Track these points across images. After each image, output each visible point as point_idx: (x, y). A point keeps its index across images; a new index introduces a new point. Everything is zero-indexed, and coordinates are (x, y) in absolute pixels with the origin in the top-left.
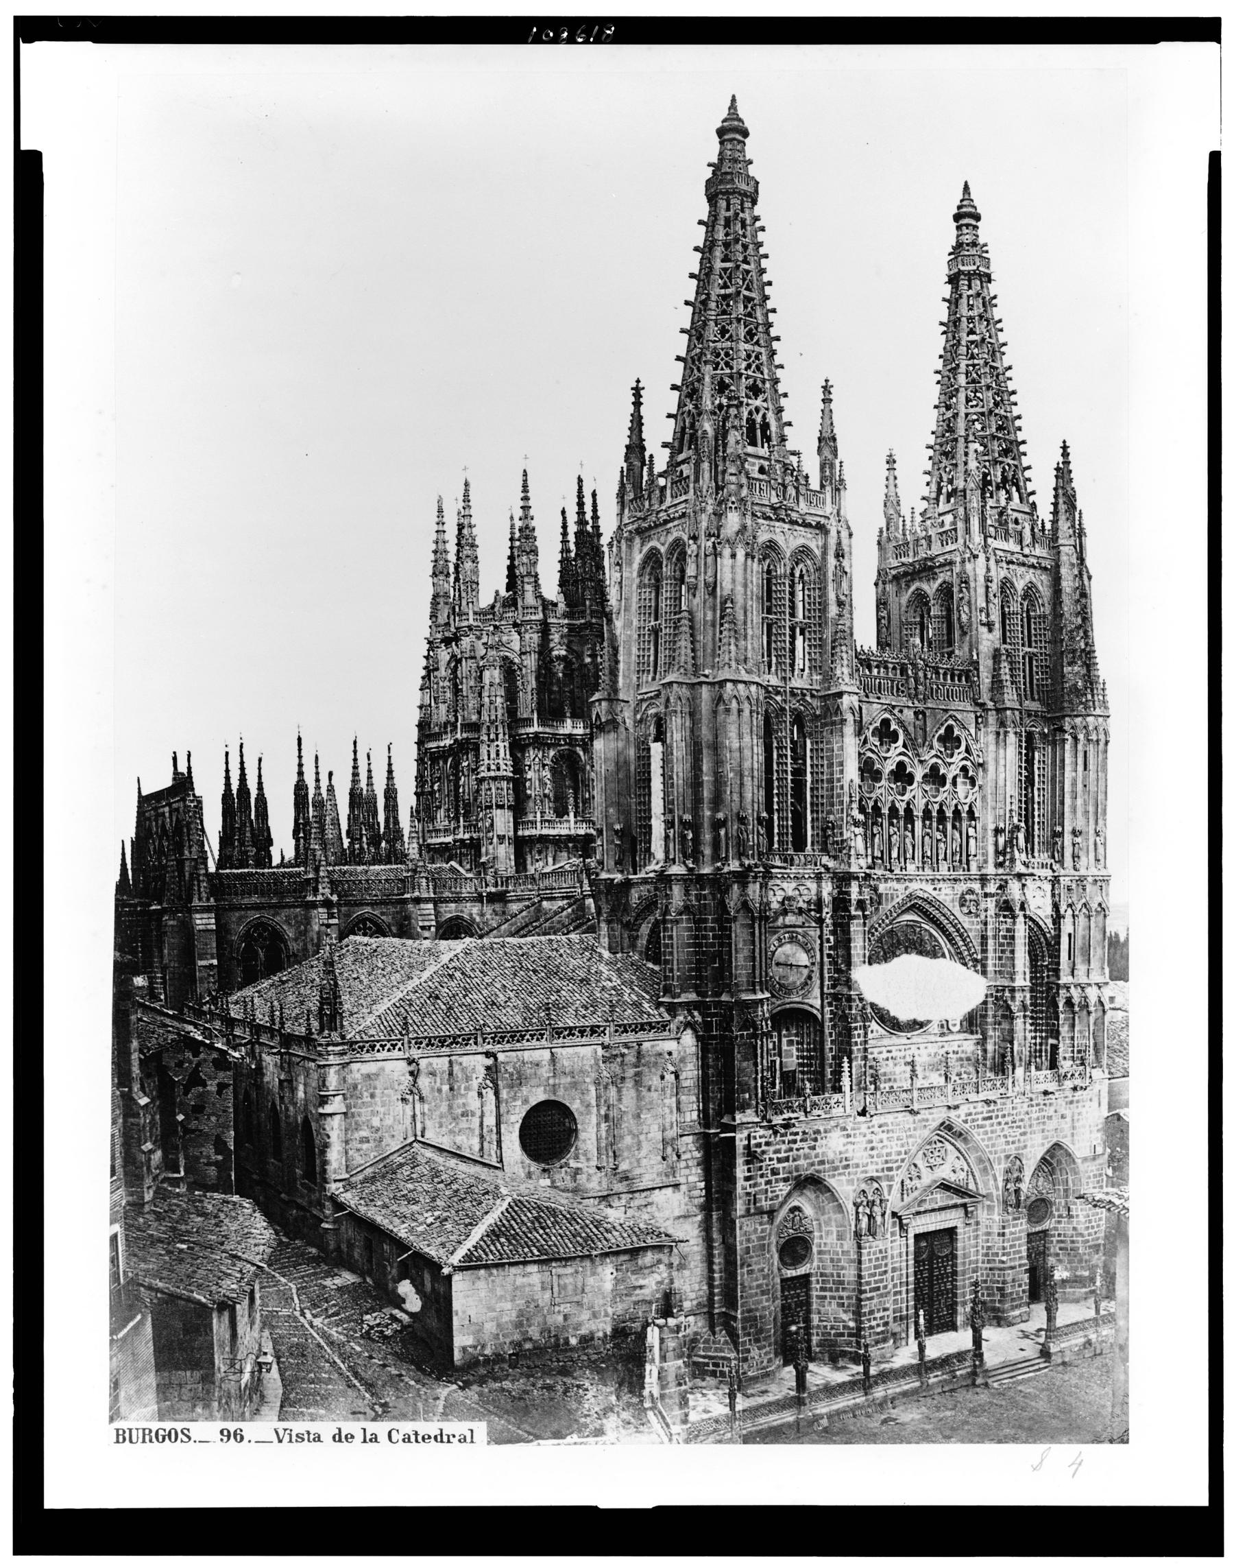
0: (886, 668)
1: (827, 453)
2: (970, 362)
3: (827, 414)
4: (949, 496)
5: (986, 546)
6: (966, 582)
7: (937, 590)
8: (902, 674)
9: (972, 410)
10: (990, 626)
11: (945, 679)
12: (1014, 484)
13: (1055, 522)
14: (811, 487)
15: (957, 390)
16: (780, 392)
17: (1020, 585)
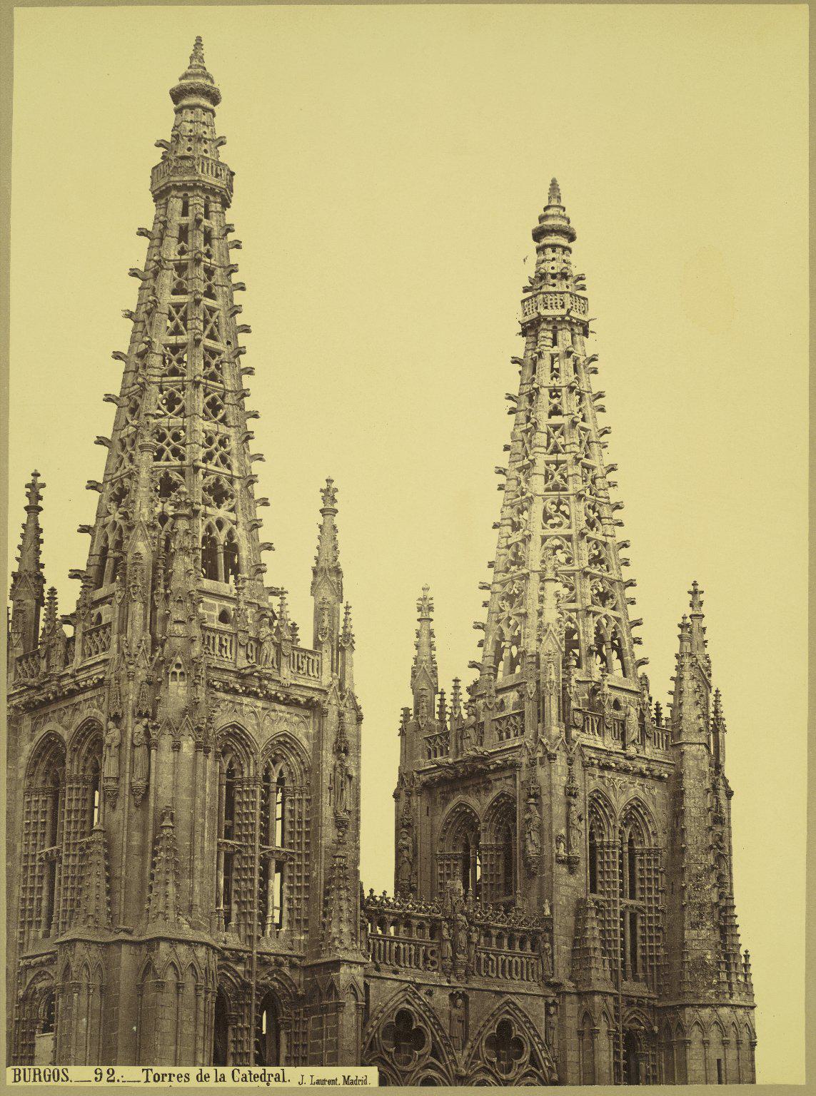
0: (408, 925)
1: (326, 593)
2: (553, 458)
3: (328, 533)
4: (513, 663)
5: (569, 739)
6: (536, 796)
7: (491, 807)
8: (432, 936)
9: (551, 532)
10: (571, 864)
11: (500, 945)
12: (614, 647)
13: (676, 707)
14: (301, 644)
15: (530, 500)
16: (257, 497)
17: (619, 802)
